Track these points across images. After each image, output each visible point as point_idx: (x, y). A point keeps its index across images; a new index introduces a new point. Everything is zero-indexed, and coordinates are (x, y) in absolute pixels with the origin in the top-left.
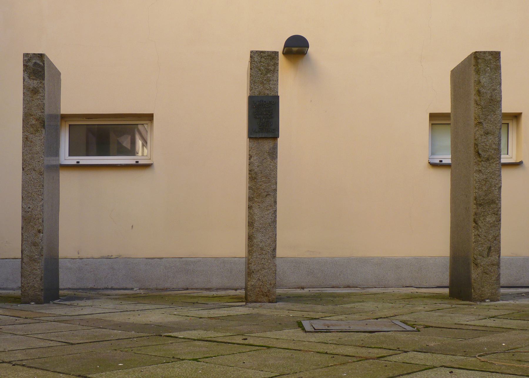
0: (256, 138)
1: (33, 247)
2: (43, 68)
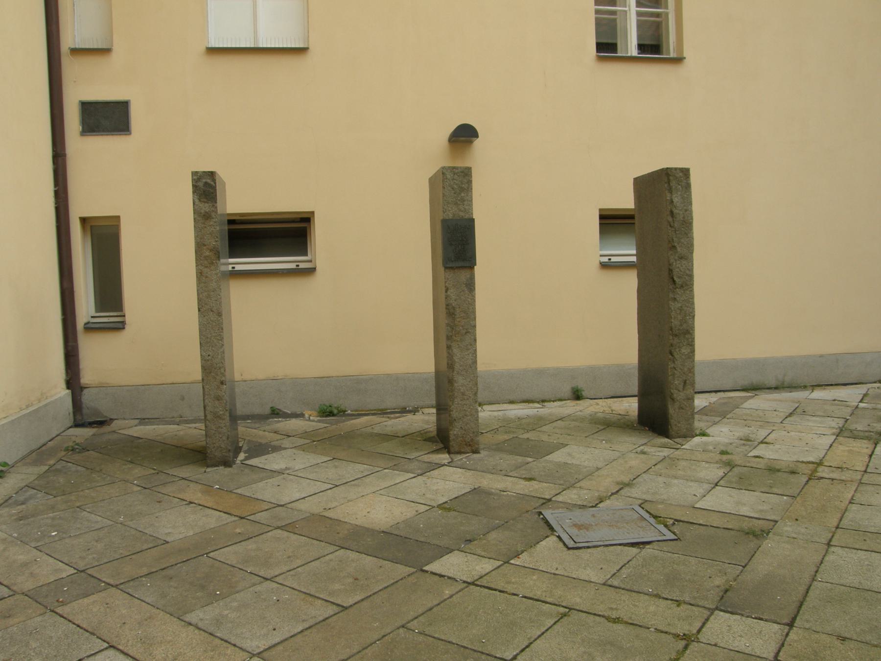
0: (452, 268)
1: (217, 402)
2: (214, 188)
